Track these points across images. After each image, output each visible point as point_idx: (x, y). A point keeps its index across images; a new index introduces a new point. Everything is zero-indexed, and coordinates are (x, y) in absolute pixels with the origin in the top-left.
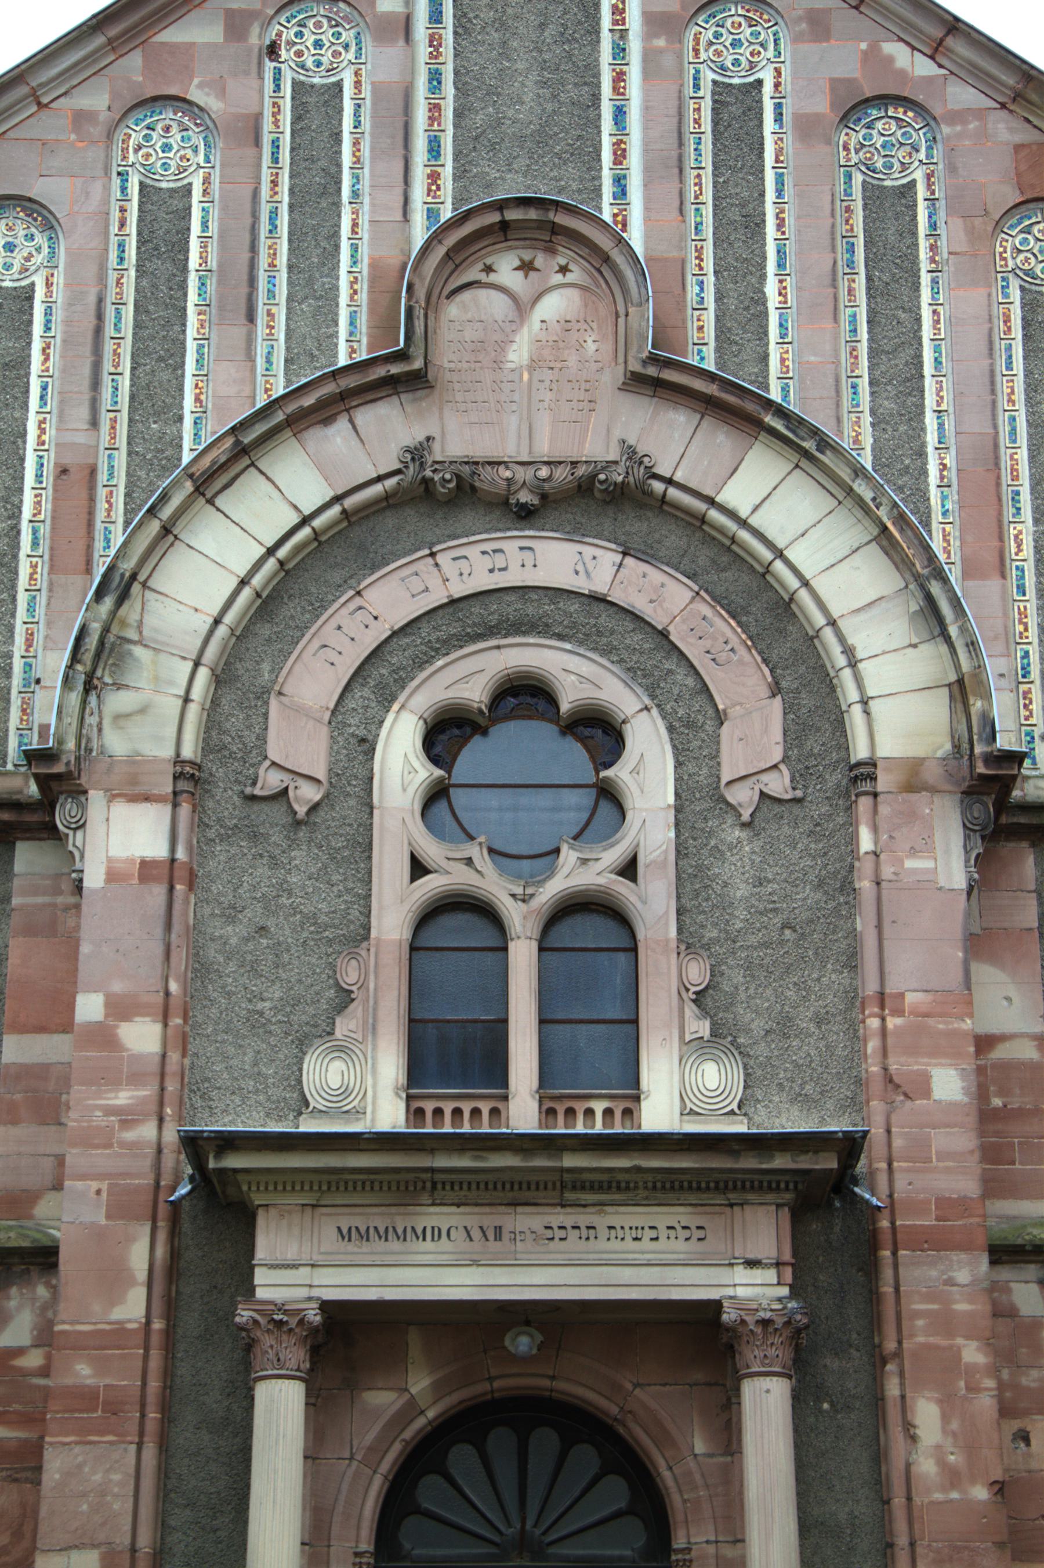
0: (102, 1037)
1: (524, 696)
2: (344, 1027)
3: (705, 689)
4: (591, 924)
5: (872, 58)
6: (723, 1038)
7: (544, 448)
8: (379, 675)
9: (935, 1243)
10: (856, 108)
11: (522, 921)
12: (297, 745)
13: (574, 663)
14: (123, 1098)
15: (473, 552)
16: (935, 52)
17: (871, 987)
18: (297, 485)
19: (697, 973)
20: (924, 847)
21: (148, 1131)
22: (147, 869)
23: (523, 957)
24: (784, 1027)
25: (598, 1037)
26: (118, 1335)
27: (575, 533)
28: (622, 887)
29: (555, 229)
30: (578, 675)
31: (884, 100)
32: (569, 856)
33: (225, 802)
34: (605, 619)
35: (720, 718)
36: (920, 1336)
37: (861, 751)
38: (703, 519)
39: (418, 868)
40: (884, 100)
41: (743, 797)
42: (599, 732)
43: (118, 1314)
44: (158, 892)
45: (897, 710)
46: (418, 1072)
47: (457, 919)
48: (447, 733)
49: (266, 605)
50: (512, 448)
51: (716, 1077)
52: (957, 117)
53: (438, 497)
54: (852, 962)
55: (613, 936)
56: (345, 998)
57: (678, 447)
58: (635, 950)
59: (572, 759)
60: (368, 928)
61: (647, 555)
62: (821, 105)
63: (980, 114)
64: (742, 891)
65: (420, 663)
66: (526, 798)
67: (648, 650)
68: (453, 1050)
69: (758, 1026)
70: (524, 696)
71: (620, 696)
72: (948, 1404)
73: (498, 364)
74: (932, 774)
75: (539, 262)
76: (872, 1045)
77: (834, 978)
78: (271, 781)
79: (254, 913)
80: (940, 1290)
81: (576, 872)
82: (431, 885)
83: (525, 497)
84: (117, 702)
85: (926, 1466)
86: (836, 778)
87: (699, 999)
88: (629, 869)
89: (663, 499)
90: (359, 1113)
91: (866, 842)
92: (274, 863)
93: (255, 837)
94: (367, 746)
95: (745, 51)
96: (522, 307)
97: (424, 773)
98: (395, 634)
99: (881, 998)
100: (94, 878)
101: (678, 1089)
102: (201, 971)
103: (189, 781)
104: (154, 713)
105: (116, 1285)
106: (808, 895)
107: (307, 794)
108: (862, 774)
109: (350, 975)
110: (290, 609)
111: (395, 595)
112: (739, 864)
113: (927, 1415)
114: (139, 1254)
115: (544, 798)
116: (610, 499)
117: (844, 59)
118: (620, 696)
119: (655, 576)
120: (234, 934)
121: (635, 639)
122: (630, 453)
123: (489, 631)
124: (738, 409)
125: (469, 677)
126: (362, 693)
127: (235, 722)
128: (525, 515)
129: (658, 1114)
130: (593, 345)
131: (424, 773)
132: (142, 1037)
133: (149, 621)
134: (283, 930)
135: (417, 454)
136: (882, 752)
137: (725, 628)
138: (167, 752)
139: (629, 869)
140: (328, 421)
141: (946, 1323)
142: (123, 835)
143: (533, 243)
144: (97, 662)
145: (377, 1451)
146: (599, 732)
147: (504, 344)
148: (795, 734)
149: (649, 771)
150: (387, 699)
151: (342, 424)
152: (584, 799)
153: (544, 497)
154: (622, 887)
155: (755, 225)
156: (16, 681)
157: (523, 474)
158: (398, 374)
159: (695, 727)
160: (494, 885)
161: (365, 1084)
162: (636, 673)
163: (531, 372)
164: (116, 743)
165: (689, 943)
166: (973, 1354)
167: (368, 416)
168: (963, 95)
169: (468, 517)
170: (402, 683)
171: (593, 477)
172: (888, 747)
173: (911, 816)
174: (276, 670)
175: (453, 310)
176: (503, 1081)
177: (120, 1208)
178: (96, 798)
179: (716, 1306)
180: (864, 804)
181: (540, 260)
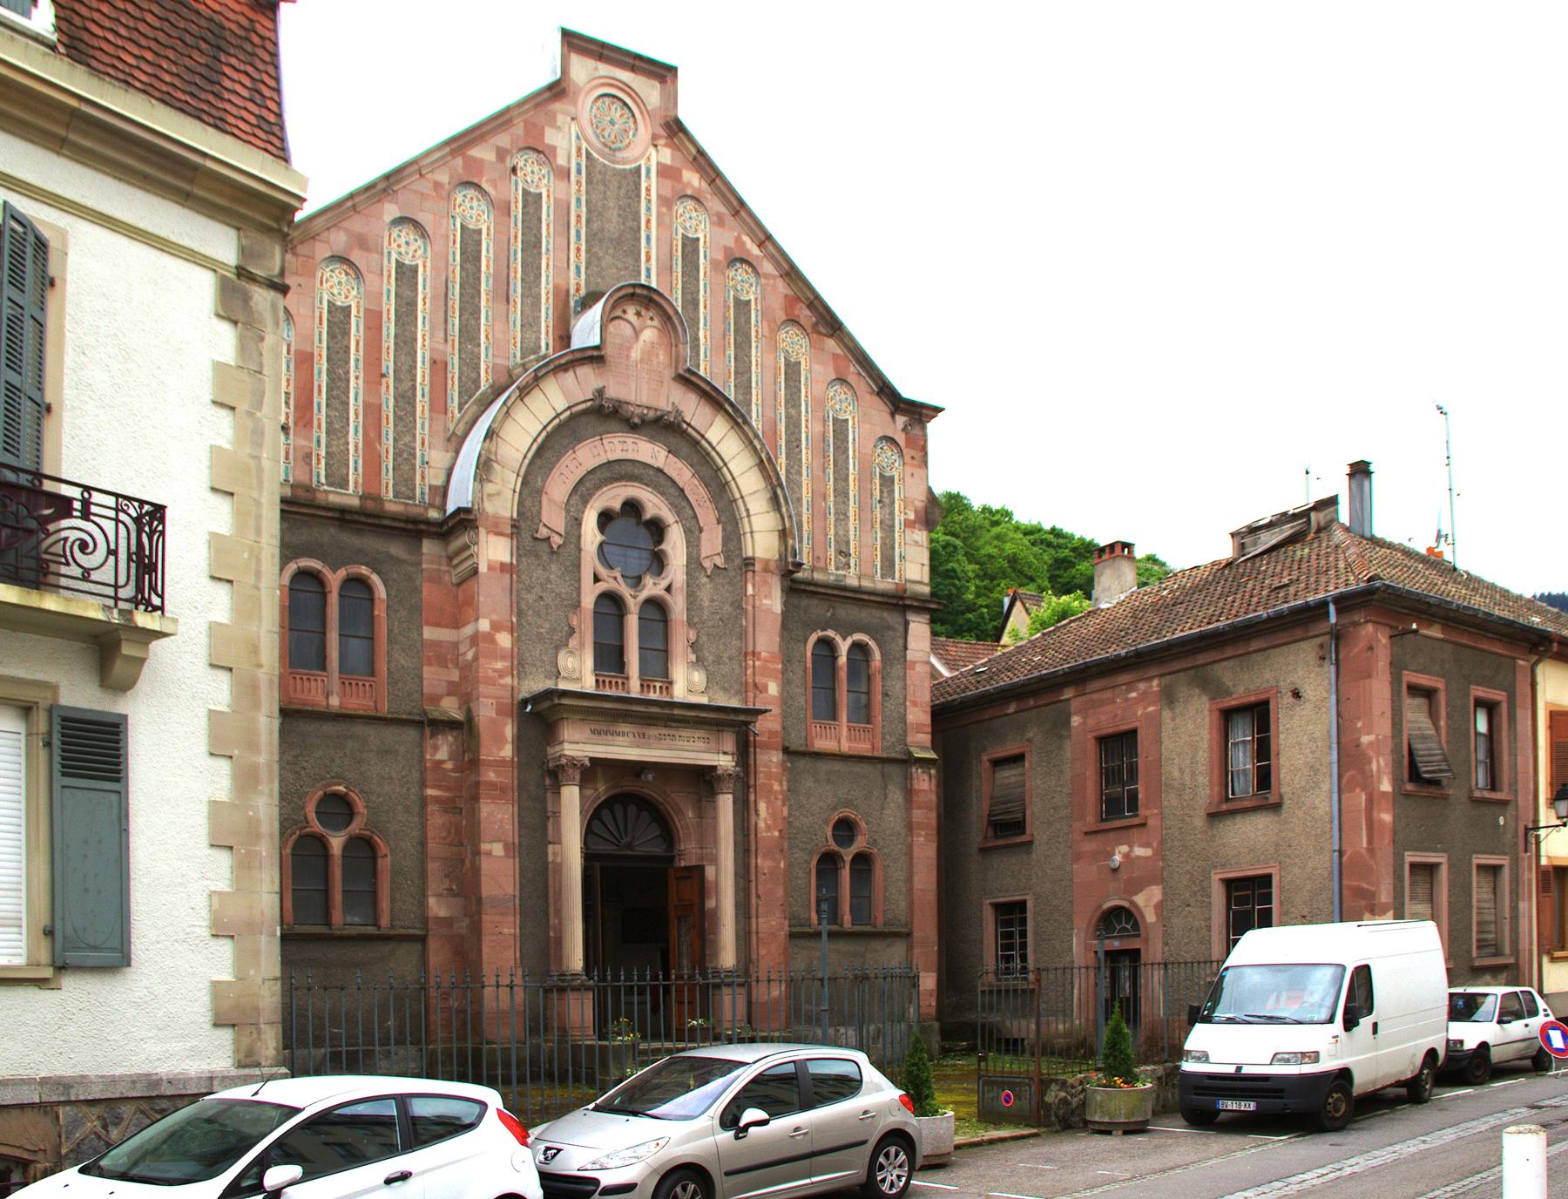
2: (573, 642)
3: (696, 517)
4: (657, 608)
6: (699, 662)
7: (644, 399)
8: (583, 490)
11: (633, 604)
12: (553, 518)
13: (652, 497)
15: (616, 441)
17: (750, 649)
19: (693, 636)
22: (504, 567)
23: (632, 622)
24: (718, 660)
28: (667, 596)
29: (651, 300)
30: (654, 505)
32: (649, 580)
33: (526, 536)
34: (662, 480)
35: (701, 530)
37: (750, 554)
38: (698, 443)
39: (597, 579)
41: (707, 564)
42: (657, 529)
43: (502, 754)
45: (762, 541)
47: (611, 603)
50: (632, 399)
51: (699, 677)
53: (605, 414)
54: (742, 636)
56: (572, 631)
60: (579, 602)
62: (720, 256)
63: (774, 277)
64: (706, 604)
65: (598, 488)
67: (678, 497)
68: (610, 658)
69: (711, 658)
71: (668, 516)
73: (628, 357)
74: (772, 566)
75: (643, 312)
76: (750, 671)
77: (736, 643)
78: (543, 532)
79: (538, 590)
81: (652, 587)
83: (636, 420)
86: (737, 561)
89: (685, 431)
90: (579, 680)
91: (750, 591)
92: (545, 569)
93: (537, 556)
95: (694, 222)
96: (637, 333)
97: (599, 538)
98: (590, 473)
99: (754, 653)
101: (687, 683)
102: (520, 614)
108: (749, 562)
109: (575, 623)
110: (548, 454)
111: (589, 455)
118: (668, 516)
119: (680, 464)
120: (531, 597)
121: (672, 490)
124: (713, 398)
125: (613, 496)
126: (576, 498)
127: (528, 503)
129: (680, 693)
130: (662, 357)
131: (599, 538)
133: (500, 452)
134: (549, 598)
135: (600, 392)
136: (758, 555)
137: (702, 490)
138: (508, 515)
139: (668, 589)
140: (566, 370)
143: (641, 303)
146: (657, 529)
147: (629, 349)
149: (675, 545)
150: (585, 502)
151: (571, 373)
153: (643, 421)
156: (418, 462)
157: (638, 411)
159: (693, 533)
160: (624, 590)
161: (578, 670)
165: (690, 623)
169: (613, 424)
170: (591, 496)
171: (661, 417)
172: (759, 554)
173: (765, 582)
174: (544, 481)
175: (611, 328)
179: (715, 767)
180: (750, 575)
181: (643, 312)
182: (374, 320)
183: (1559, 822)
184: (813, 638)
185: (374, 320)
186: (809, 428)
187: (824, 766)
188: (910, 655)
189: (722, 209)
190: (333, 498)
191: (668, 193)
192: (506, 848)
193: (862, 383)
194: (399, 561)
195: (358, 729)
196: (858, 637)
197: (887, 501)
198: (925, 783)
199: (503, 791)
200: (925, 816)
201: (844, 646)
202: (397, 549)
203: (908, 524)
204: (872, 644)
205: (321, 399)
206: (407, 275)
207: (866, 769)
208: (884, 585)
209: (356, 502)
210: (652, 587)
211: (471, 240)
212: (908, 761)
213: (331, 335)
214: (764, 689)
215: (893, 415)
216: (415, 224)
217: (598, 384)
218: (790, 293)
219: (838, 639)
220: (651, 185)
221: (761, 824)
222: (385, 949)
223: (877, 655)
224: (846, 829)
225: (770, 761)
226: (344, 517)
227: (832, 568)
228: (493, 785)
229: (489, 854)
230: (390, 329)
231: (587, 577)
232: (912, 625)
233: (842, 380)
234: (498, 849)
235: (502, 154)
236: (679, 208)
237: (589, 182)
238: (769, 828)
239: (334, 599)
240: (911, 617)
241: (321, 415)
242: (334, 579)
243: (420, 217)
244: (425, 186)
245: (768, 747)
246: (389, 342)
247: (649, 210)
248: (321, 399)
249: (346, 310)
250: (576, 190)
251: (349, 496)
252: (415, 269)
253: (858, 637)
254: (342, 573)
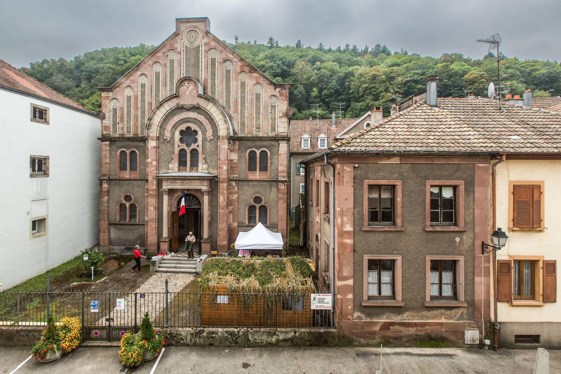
0: (151, 163)
2: (173, 161)
4: (194, 153)
6: (206, 162)
7: (190, 103)
8: (175, 127)
9: (223, 182)
10: (225, 61)
12: (168, 135)
14: (153, 168)
18: (167, 107)
19: (204, 156)
20: (224, 145)
21: (155, 172)
24: (211, 161)
26: (154, 189)
27: (193, 112)
30: (194, 127)
31: (228, 60)
33: (161, 140)
36: (221, 190)
39: (179, 146)
40: (228, 60)
41: (208, 139)
44: (155, 149)
48: (182, 132)
49: (165, 120)
53: (180, 108)
56: (172, 159)
57: (202, 103)
61: (200, 114)
62: (221, 61)
64: (208, 148)
67: (200, 124)
72: (223, 196)
78: (165, 138)
79: (164, 151)
80: (223, 186)
81: (193, 146)
82: (180, 148)
84: (151, 130)
85: (221, 201)
88: (198, 146)
94: (174, 134)
96: (188, 88)
100: (150, 148)
103: (158, 138)
104: (154, 132)
105: (152, 186)
106: (214, 149)
107: (169, 139)
108: (219, 137)
110: (167, 120)
111: (177, 118)
112: (208, 145)
113: (221, 197)
114: (155, 183)
116: (196, 108)
117: (224, 56)
118: (197, 128)
120: (163, 153)
122: (198, 103)
123: (185, 122)
124: (208, 99)
125: (183, 127)
128: (188, 110)
132: (154, 163)
134: (167, 152)
135: (177, 104)
139: (198, 146)
141: (223, 189)
142: (152, 144)
144: (149, 127)
145: (176, 199)
148: (213, 132)
149: (200, 137)
155: (215, 74)
158: (176, 96)
163: (189, 95)
164: (151, 135)
165: (203, 153)
166: (225, 192)
167: (173, 100)
169: (183, 110)
175: (181, 88)
176: (186, 166)
177: (153, 179)
178: (149, 140)
182: (136, 97)
184: (248, 151)
185: (136, 97)
186: (248, 97)
187: (251, 183)
188: (280, 152)
189: (222, 49)
190: (128, 136)
191: (207, 49)
193: (265, 82)
194: (142, 146)
195: (133, 182)
196: (262, 149)
197: (273, 112)
201: (258, 152)
202: (141, 144)
203: (280, 117)
204: (267, 151)
205: (125, 116)
206: (143, 86)
207: (265, 183)
208: (273, 134)
209: (132, 136)
210: (193, 146)
211: (157, 74)
213: (127, 102)
214: (222, 168)
215: (275, 89)
216: (145, 75)
217: (177, 102)
218: (242, 64)
219: (256, 150)
220: (203, 49)
222: (137, 227)
223: (269, 153)
226: (129, 139)
227: (255, 133)
230: (140, 98)
231: (176, 146)
232: (281, 145)
233: (258, 83)
235: (164, 53)
236: (210, 52)
237: (186, 53)
239: (128, 156)
240: (280, 142)
241: (125, 120)
242: (128, 152)
243: (145, 73)
244: (146, 66)
246: (139, 101)
247: (202, 55)
248: (125, 116)
249: (130, 97)
250: (183, 55)
251: (131, 135)
252: (145, 84)
253: (262, 149)
254: (130, 150)
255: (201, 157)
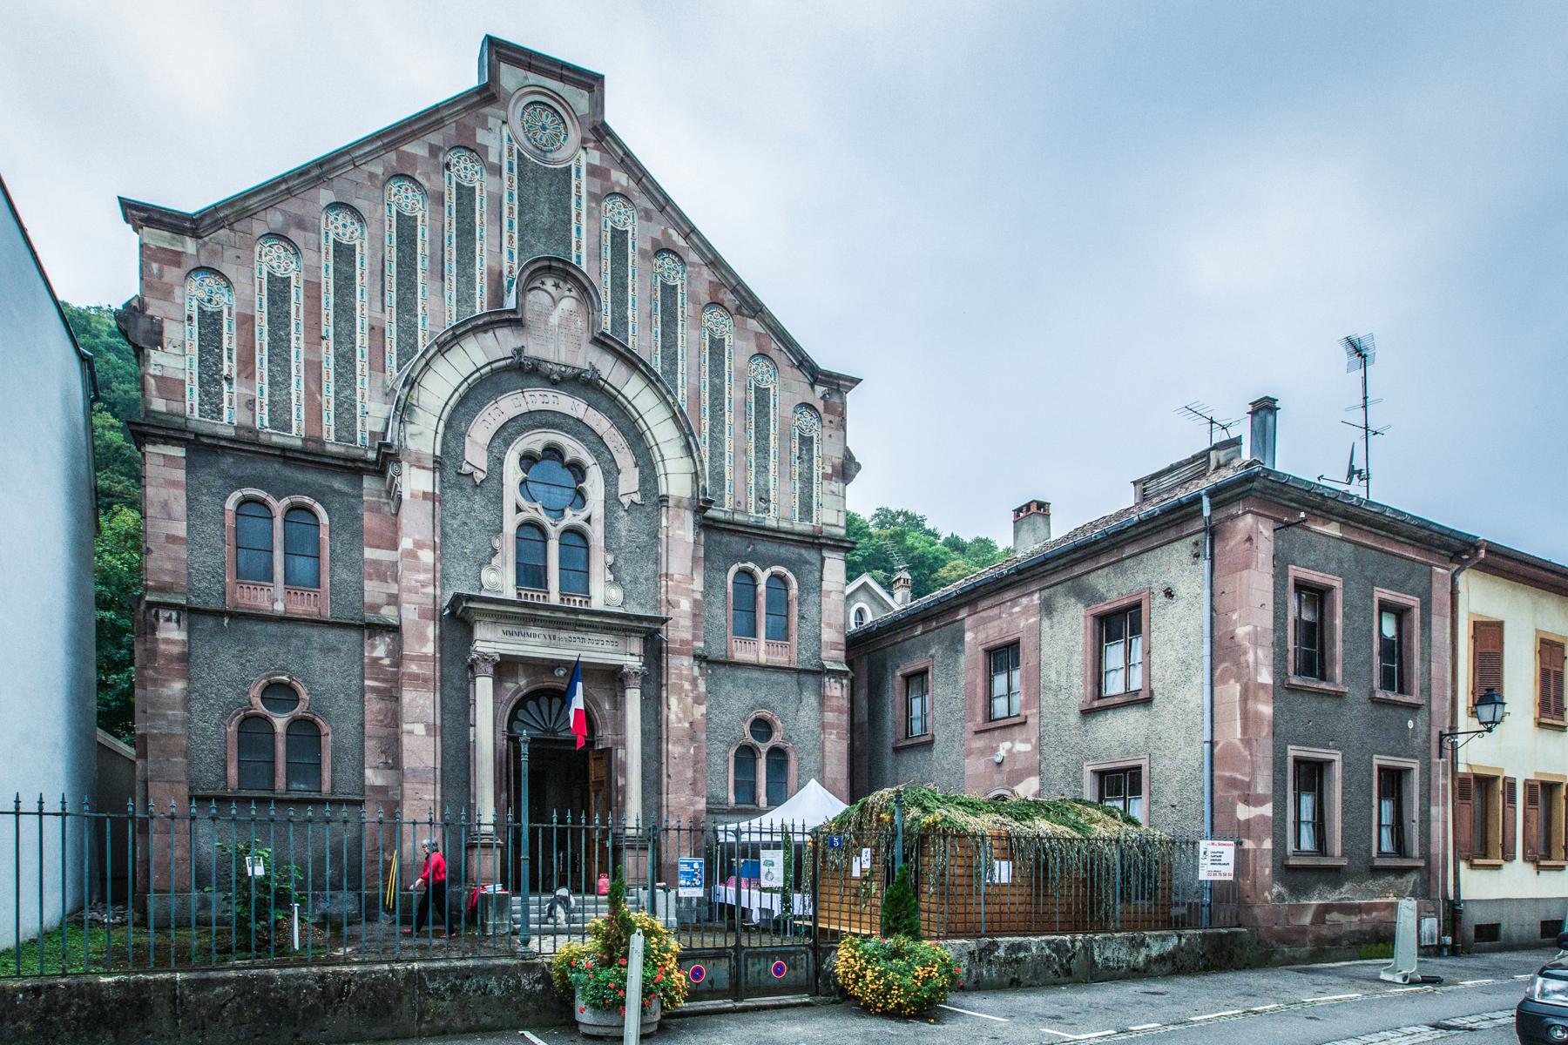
1: (553, 451)
4: (576, 537)
5: (665, 232)
6: (617, 580)
7: (563, 360)
11: (554, 533)
13: (572, 443)
16: (686, 237)
19: (610, 559)
24: (635, 580)
25: (576, 574)
27: (572, 394)
28: (586, 525)
30: (574, 449)
32: (569, 512)
34: (582, 429)
39: (519, 510)
42: (578, 469)
46: (519, 582)
47: (532, 531)
50: (551, 357)
52: (692, 264)
54: (657, 561)
55: (580, 543)
56: (494, 552)
58: (587, 548)
59: (567, 477)
66: (554, 489)
68: (532, 575)
70: (553, 451)
73: (546, 322)
77: (652, 567)
81: (572, 518)
82: (523, 516)
87: (610, 568)
88: (588, 520)
96: (555, 302)
97: (521, 475)
115: (558, 490)
125: (535, 441)
128: (554, 384)
131: (521, 475)
139: (588, 520)
147: (548, 315)
152: (570, 492)
154: (586, 525)
157: (556, 368)
160: (545, 519)
162: (592, 451)
168: (693, 257)
183: (1482, 728)
192: (428, 727)
198: (836, 691)
199: (425, 681)
200: (837, 718)
212: (820, 672)
221: (672, 717)
224: (762, 727)
225: (680, 667)
228: (416, 677)
229: (411, 733)
234: (420, 729)
238: (680, 721)
245: (680, 653)
255: (599, 561)
